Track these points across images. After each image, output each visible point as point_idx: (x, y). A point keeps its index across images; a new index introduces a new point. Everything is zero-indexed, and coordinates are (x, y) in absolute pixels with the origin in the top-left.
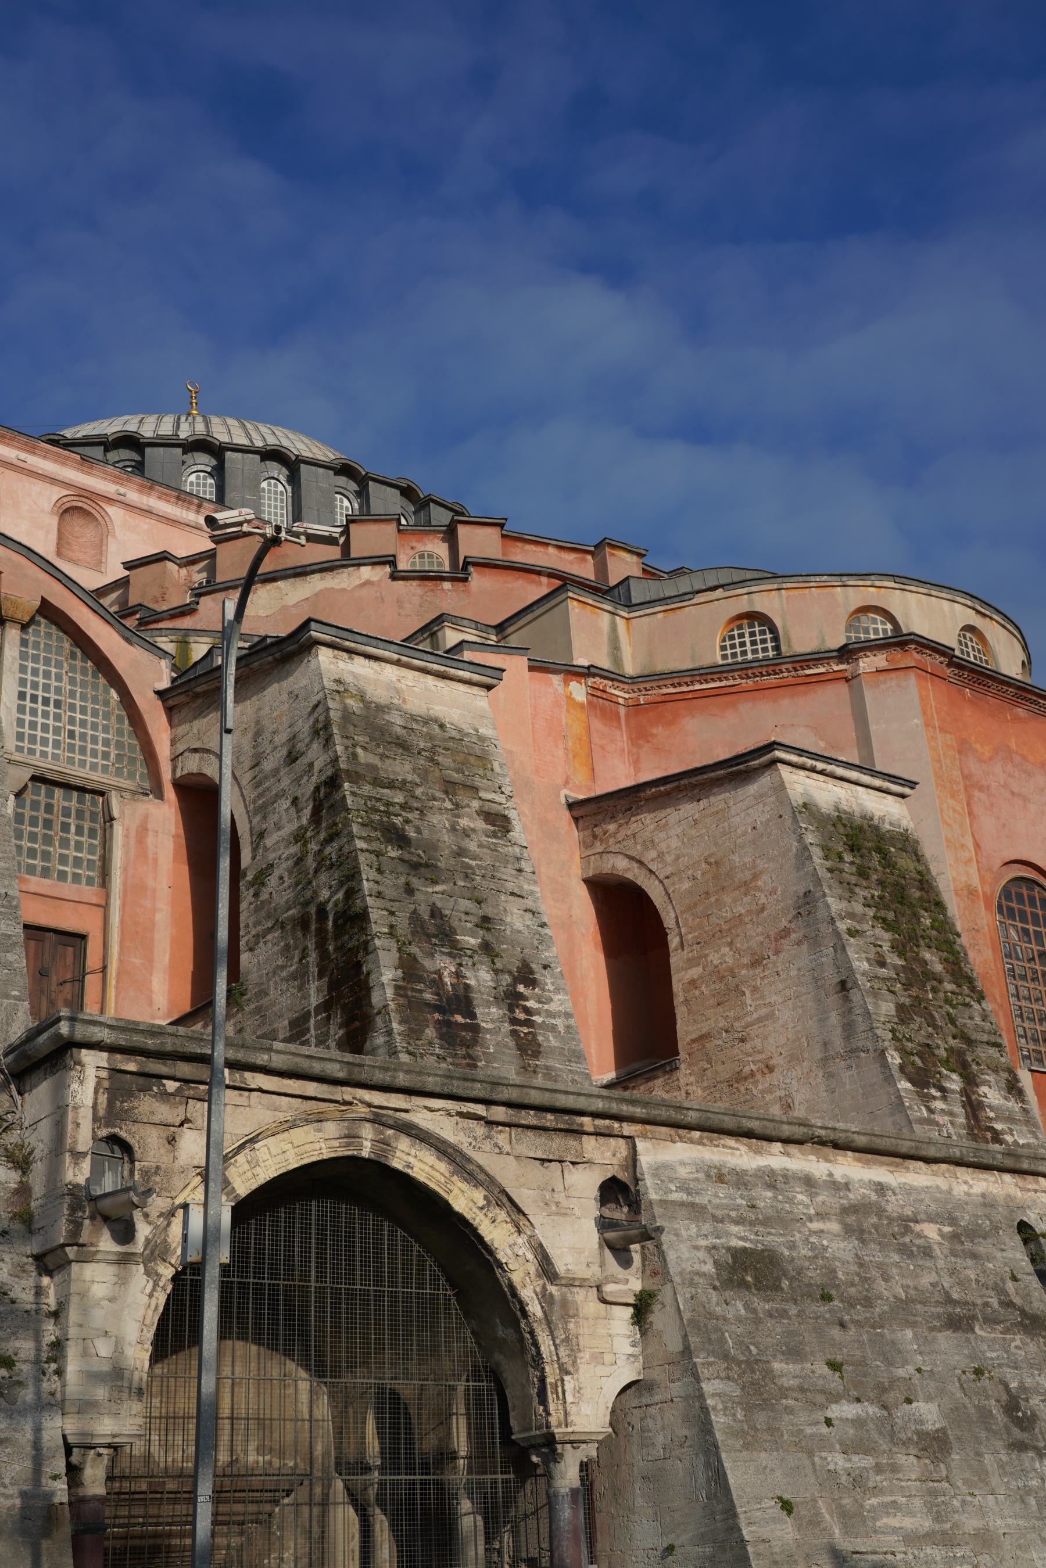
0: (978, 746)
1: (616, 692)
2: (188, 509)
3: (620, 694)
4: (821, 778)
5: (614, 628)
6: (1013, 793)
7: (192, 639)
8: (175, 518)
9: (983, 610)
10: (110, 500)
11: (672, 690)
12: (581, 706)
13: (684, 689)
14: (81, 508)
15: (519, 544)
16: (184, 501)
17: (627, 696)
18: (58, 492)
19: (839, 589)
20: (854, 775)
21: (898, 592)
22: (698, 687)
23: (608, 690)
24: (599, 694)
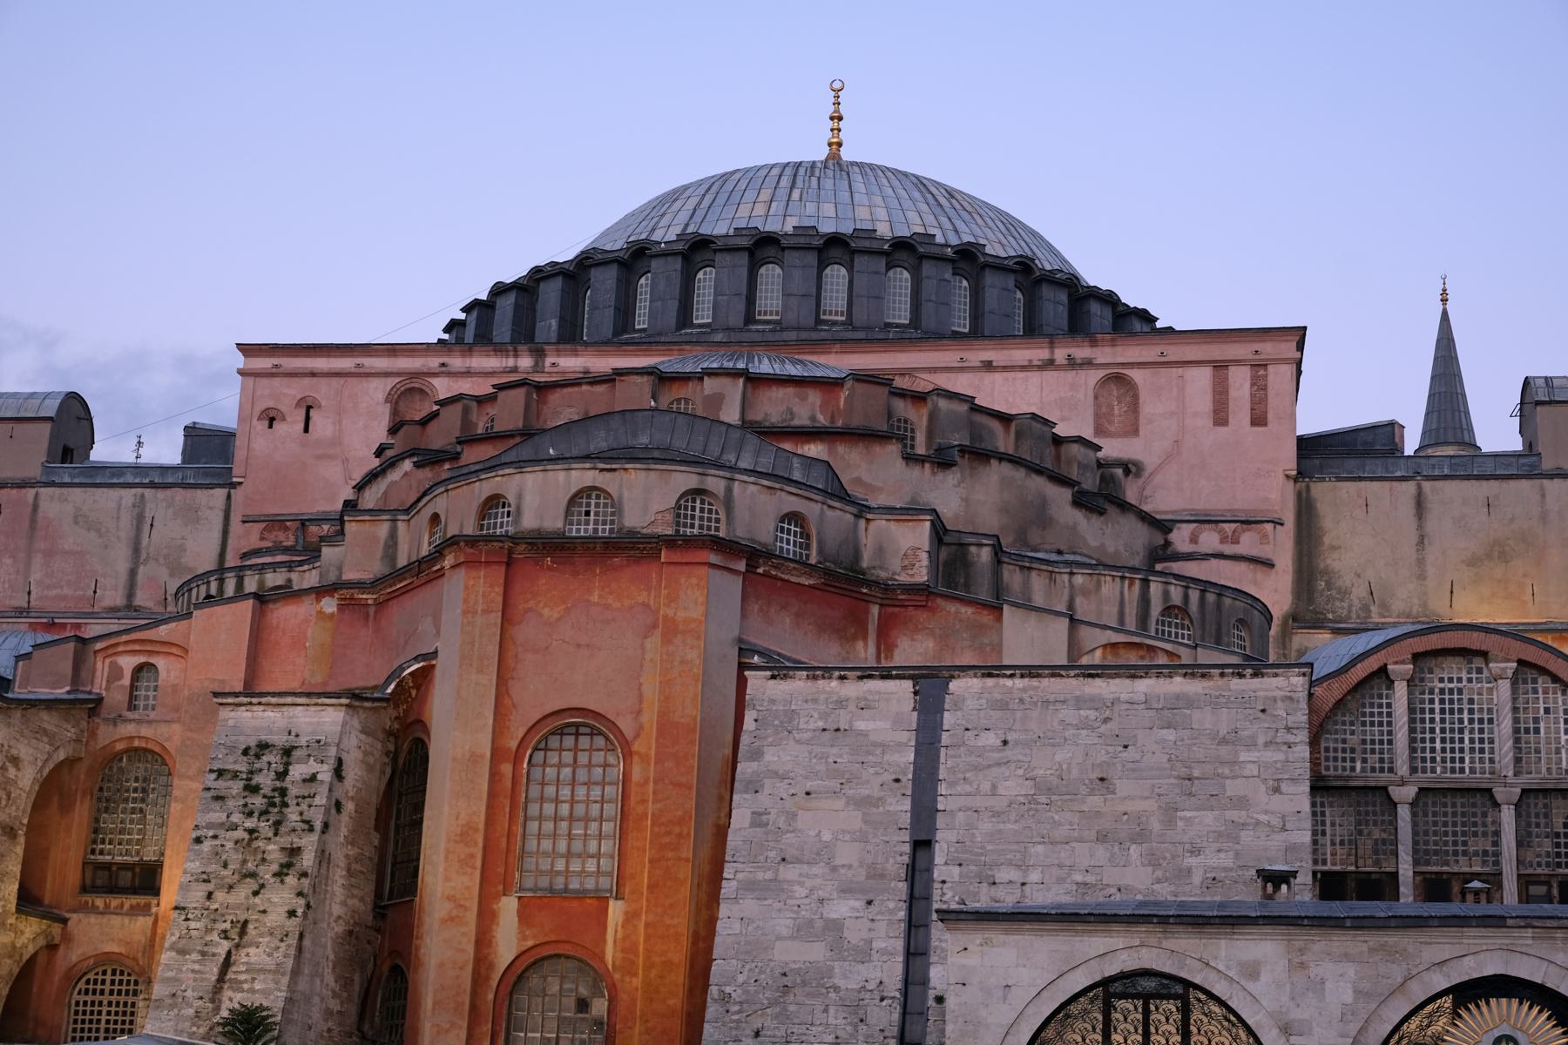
0: (546, 612)
1: (364, 596)
2: (507, 356)
3: (369, 597)
4: (262, 708)
5: (393, 534)
6: (579, 646)
7: (227, 575)
8: (491, 370)
9: (608, 466)
10: (435, 375)
11: (389, 590)
12: (332, 615)
13: (394, 588)
14: (413, 388)
15: (558, 390)
16: (501, 351)
17: (374, 596)
18: (391, 382)
19: (478, 483)
20: (289, 700)
21: (518, 475)
22: (398, 586)
23: (356, 596)
24: (347, 602)
